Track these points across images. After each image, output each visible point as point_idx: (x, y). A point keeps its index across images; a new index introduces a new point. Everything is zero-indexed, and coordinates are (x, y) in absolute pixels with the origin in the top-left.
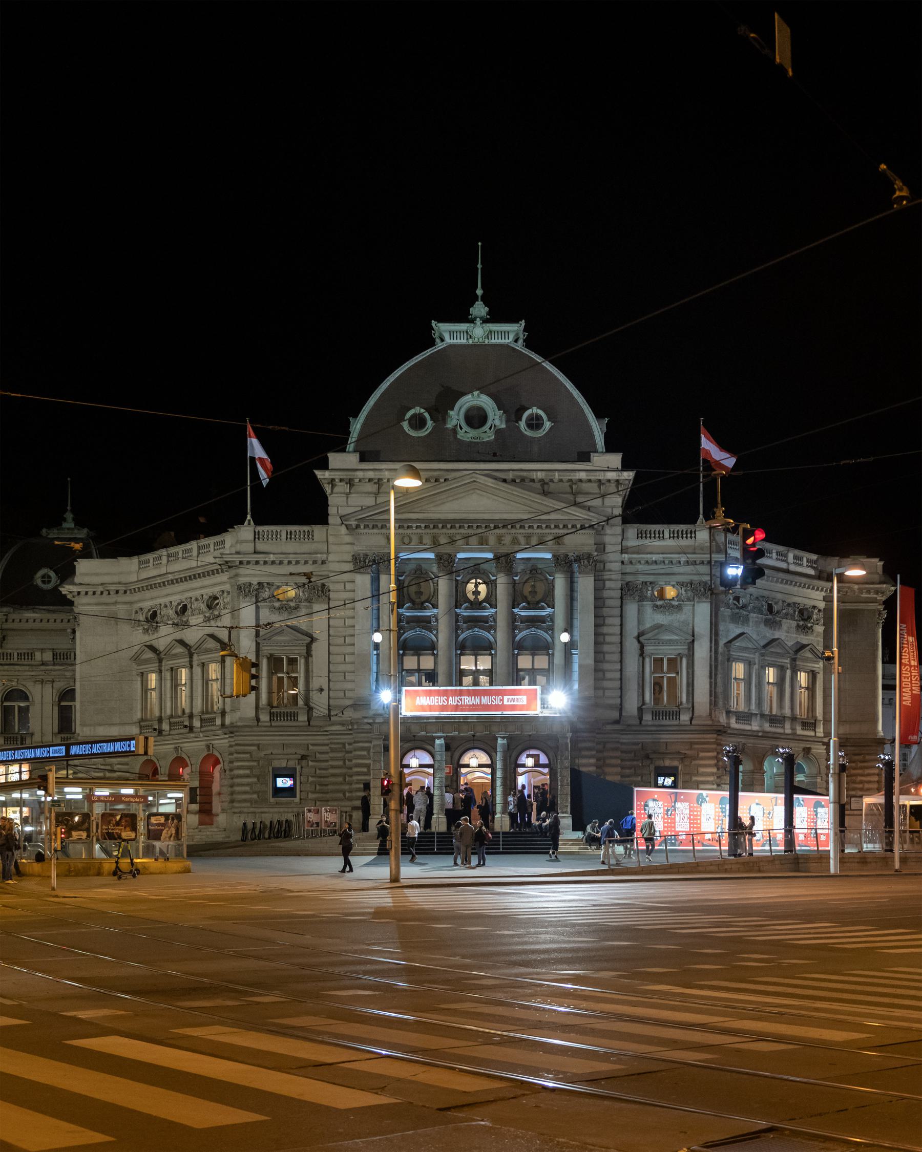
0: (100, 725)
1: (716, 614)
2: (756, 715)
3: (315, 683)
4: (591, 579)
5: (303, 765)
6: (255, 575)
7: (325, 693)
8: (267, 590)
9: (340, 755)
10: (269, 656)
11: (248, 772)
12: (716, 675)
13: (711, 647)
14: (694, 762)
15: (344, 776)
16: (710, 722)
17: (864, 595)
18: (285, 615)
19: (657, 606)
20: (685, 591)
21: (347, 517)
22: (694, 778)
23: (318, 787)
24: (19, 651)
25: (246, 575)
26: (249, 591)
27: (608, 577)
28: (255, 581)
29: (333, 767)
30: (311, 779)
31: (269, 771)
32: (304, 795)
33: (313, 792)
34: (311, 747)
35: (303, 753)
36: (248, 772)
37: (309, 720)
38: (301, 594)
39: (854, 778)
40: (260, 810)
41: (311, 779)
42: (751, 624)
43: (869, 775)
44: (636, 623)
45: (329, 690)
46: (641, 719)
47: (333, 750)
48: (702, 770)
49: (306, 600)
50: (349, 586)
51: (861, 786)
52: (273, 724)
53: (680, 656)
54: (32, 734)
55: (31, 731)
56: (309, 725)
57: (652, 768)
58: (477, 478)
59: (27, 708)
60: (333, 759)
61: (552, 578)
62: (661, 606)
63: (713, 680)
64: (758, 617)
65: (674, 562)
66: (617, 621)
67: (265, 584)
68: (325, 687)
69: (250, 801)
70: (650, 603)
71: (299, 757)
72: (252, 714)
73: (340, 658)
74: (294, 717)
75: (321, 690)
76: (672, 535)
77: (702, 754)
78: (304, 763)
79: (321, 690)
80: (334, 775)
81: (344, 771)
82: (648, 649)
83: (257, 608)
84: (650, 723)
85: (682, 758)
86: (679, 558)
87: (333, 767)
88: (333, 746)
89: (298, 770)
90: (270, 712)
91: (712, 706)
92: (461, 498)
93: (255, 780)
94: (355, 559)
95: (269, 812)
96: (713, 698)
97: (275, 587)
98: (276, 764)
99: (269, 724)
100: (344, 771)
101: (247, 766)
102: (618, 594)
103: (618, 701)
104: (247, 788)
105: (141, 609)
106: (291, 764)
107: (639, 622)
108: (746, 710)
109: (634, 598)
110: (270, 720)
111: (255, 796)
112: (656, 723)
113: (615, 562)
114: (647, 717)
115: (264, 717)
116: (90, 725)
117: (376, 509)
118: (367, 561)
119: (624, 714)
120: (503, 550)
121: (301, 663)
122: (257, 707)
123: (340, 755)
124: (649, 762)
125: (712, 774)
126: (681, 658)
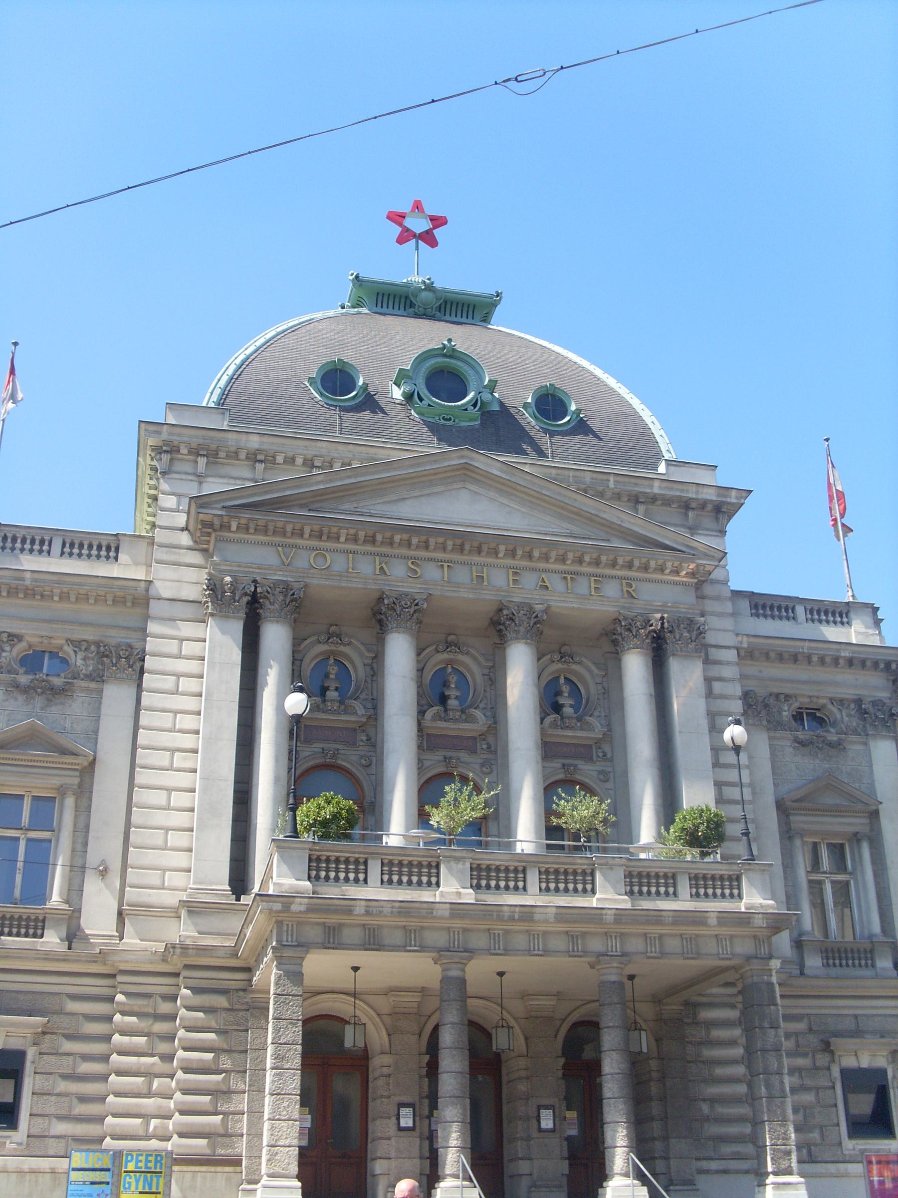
18: (39, 701)
20: (849, 715)
27: (717, 675)
32: (39, 1125)
45: (125, 866)
53: (856, 838)
57: (836, 1072)
58: (472, 459)
68: (115, 865)
70: (788, 734)
73: (159, 798)
75: (104, 873)
76: (809, 616)
92: (437, 493)
97: (23, 644)
106: (14, 1044)
109: (761, 720)
124: (822, 1059)
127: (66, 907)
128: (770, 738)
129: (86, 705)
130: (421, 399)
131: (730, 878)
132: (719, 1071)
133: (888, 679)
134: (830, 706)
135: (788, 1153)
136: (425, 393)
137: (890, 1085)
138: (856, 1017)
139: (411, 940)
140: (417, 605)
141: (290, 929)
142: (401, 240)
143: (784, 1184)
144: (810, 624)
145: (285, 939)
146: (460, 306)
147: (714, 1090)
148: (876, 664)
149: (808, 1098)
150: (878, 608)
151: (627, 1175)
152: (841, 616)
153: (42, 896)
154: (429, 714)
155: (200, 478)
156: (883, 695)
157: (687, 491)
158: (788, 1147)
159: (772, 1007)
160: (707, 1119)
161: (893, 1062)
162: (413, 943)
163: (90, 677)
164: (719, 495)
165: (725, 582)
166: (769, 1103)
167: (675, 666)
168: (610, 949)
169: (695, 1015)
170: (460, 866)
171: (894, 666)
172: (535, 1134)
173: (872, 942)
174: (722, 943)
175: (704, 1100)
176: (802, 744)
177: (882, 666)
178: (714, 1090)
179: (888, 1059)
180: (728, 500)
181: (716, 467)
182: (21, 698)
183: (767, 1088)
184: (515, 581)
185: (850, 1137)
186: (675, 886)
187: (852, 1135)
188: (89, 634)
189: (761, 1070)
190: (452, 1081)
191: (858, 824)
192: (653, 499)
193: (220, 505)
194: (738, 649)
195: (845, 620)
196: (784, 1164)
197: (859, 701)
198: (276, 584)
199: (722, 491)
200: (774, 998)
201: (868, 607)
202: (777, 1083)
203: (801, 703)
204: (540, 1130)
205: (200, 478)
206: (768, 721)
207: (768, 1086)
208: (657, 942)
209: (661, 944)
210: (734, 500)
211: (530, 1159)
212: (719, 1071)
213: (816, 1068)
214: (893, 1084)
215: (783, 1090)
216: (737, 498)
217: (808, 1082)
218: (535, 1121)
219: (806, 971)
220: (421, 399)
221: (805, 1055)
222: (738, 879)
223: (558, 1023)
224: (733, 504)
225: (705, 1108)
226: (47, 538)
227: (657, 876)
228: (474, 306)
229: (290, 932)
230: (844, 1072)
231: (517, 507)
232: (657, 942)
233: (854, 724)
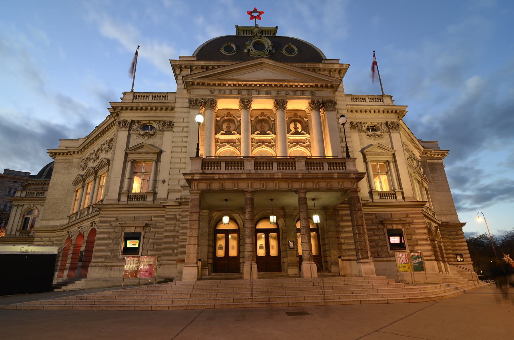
0: (52, 220)
3: (161, 178)
5: (146, 231)
6: (130, 117)
7: (166, 184)
8: (137, 125)
9: (173, 222)
10: (132, 161)
11: (106, 236)
14: (411, 226)
15: (174, 237)
17: (436, 156)
18: (147, 138)
19: (369, 136)
20: (384, 127)
21: (187, 77)
22: (414, 237)
23: (155, 247)
24: (38, 192)
25: (124, 117)
26: (125, 125)
29: (166, 231)
30: (151, 241)
31: (121, 235)
33: (151, 250)
34: (153, 218)
35: (148, 222)
36: (106, 236)
37: (154, 201)
38: (157, 127)
39: (455, 244)
40: (110, 264)
41: (151, 241)
43: (461, 242)
44: (359, 143)
46: (372, 199)
47: (167, 219)
48: (418, 231)
50: (186, 120)
51: (459, 248)
52: (129, 202)
53: (388, 162)
56: (154, 203)
57: (385, 230)
60: (167, 225)
61: (306, 120)
62: (372, 135)
65: (377, 111)
67: (136, 122)
69: (105, 257)
70: (365, 133)
71: (144, 225)
72: (116, 196)
74: (144, 198)
77: (415, 221)
78: (147, 229)
79: (164, 182)
80: (166, 237)
81: (174, 234)
82: (368, 157)
83: (129, 134)
84: (379, 201)
85: (403, 224)
86: (379, 108)
87: (166, 231)
88: (167, 216)
89: (142, 234)
90: (128, 196)
93: (111, 241)
94: (190, 101)
95: (117, 266)
98: (127, 230)
99: (126, 203)
100: (174, 234)
101: (107, 232)
104: (104, 248)
106: (138, 230)
107: (361, 144)
109: (356, 130)
110: (128, 200)
111: (109, 254)
112: (382, 200)
113: (345, 109)
114: (376, 198)
115: (124, 199)
116: (46, 220)
117: (204, 74)
118: (198, 102)
120: (279, 98)
122: (120, 194)
123: (173, 222)
124: (381, 227)
125: (425, 234)
126: (389, 163)
127: (153, 192)
128: (359, 135)
129: (159, 138)
130: (252, 51)
131: (342, 163)
133: (396, 117)
134: (378, 125)
135: (367, 252)
137: (404, 234)
138: (391, 214)
139: (234, 186)
140: (250, 102)
141: (195, 185)
142: (251, 19)
143: (365, 262)
144: (370, 102)
145: (194, 188)
146: (265, 31)
149: (377, 238)
150: (392, 97)
151: (309, 260)
152: (380, 99)
157: (330, 66)
158: (367, 250)
159: (359, 204)
160: (343, 244)
161: (404, 226)
162: (235, 187)
163: (160, 131)
164: (340, 66)
165: (343, 91)
166: (359, 235)
168: (301, 186)
169: (338, 213)
170: (251, 163)
171: (398, 111)
172: (288, 250)
173: (395, 192)
174: (340, 184)
175: (342, 238)
176: (369, 136)
177: (394, 112)
179: (402, 226)
180: (343, 68)
181: (339, 60)
182: (141, 137)
183: (358, 230)
184: (278, 94)
185: (391, 249)
186: (323, 166)
187: (391, 249)
189: (355, 224)
190: (248, 230)
191: (389, 157)
193: (191, 78)
195: (382, 101)
196: (365, 255)
197: (387, 123)
198: (209, 99)
199: (341, 65)
200: (359, 201)
201: (388, 96)
202: (362, 229)
203: (368, 125)
204: (290, 248)
206: (358, 130)
207: (358, 229)
208: (317, 184)
209: (319, 185)
210: (345, 68)
211: (287, 257)
213: (379, 229)
214: (404, 233)
215: (364, 231)
216: (346, 67)
217: (376, 233)
218: (288, 246)
219: (374, 201)
220: (252, 51)
221: (375, 225)
222: (345, 163)
223: (294, 217)
224: (344, 69)
225: (342, 241)
226: (148, 95)
227: (317, 163)
228: (270, 31)
229: (195, 186)
230: (387, 230)
231: (278, 73)
232: (317, 184)
233: (386, 129)
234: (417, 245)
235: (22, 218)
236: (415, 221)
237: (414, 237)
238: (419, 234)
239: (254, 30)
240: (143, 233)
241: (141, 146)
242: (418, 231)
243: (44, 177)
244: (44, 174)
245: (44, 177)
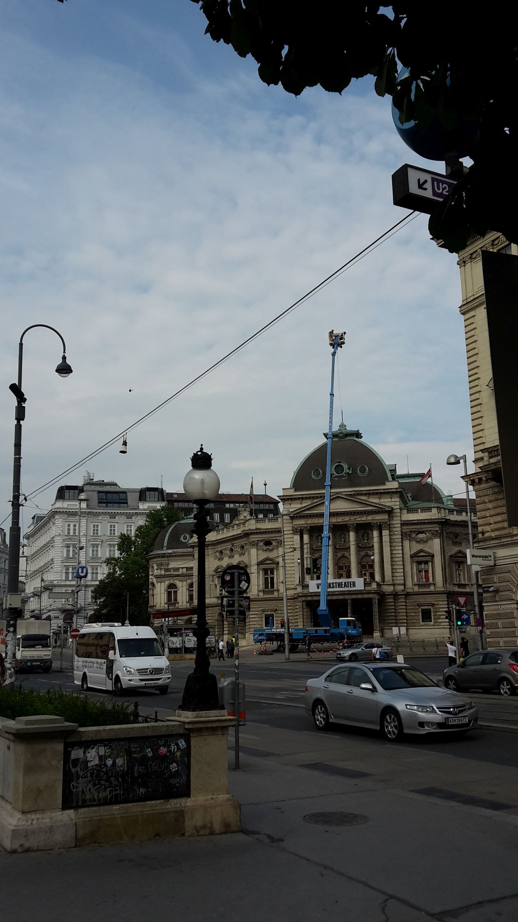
1: (443, 543)
2: (468, 585)
4: (388, 531)
12: (445, 569)
13: (441, 557)
16: (443, 589)
18: (268, 552)
22: (438, 614)
28: (257, 539)
42: (463, 545)
49: (276, 546)
54: (178, 603)
55: (178, 601)
57: (420, 610)
59: (176, 591)
63: (444, 571)
64: (466, 542)
66: (401, 548)
68: (284, 582)
75: (283, 582)
77: (440, 603)
78: (277, 612)
91: (444, 583)
96: (444, 579)
102: (400, 537)
103: (403, 582)
105: (217, 551)
108: (464, 583)
112: (420, 590)
119: (407, 587)
121: (275, 571)
124: (417, 607)
132: (389, 611)
136: (335, 473)
147: (388, 614)
148: (434, 523)
153: (274, 588)
154: (337, 546)
155: (290, 504)
156: (438, 529)
160: (387, 620)
167: (383, 531)
178: (388, 614)
187: (422, 622)
188: (275, 538)
192: (381, 493)
194: (401, 524)
196: (376, 629)
205: (290, 504)
212: (389, 611)
230: (422, 610)
234: (440, 619)
235: (166, 593)
236: (440, 603)
237: (438, 614)
238: (442, 611)
239: (339, 435)
240: (275, 614)
241: (267, 559)
242: (441, 610)
243: (165, 548)
244: (164, 545)
245: (165, 548)
